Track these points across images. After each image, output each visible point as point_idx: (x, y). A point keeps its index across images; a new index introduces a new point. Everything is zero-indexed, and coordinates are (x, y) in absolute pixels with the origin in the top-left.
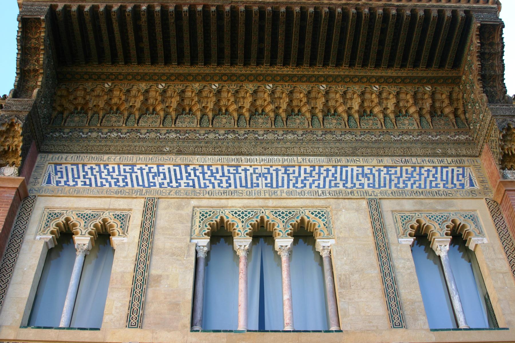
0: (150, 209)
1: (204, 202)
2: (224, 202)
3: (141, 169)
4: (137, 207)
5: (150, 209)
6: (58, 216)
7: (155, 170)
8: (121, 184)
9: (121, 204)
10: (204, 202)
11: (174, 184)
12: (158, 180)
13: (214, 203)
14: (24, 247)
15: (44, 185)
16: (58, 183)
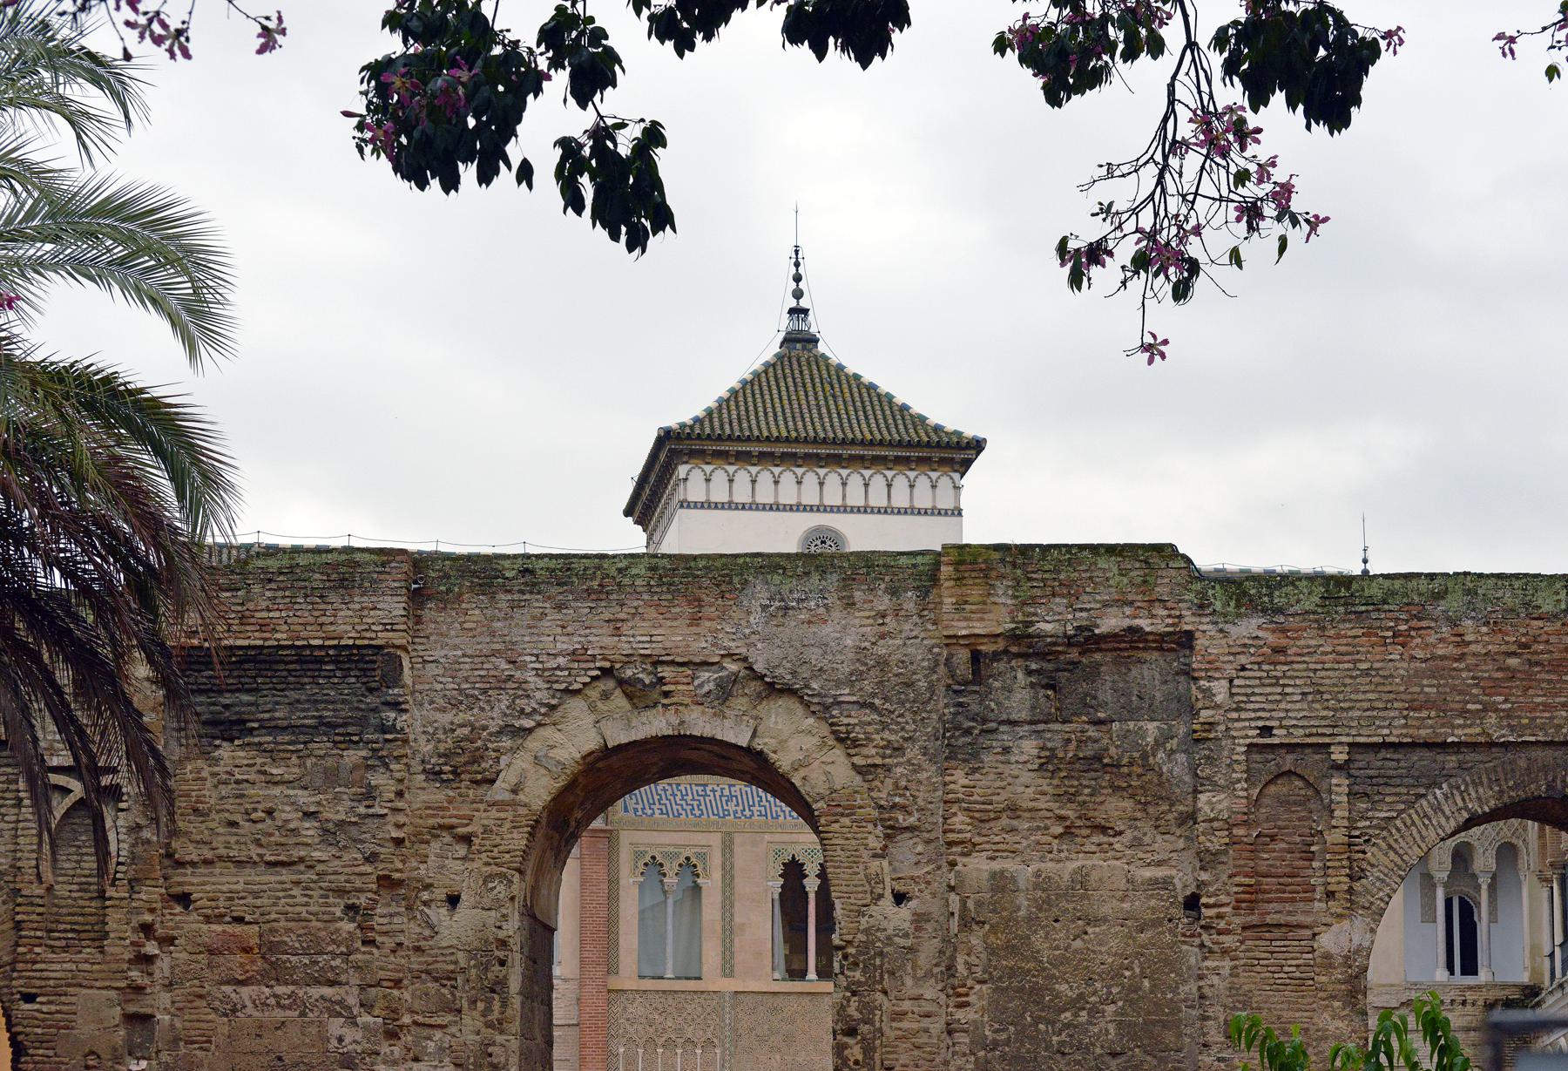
0: (728, 847)
1: (777, 838)
2: (794, 837)
3: (714, 791)
4: (715, 840)
5: (728, 847)
6: (643, 853)
7: (726, 792)
8: (697, 812)
9: (700, 839)
10: (777, 838)
11: (747, 813)
12: (731, 807)
13: (786, 838)
14: (622, 893)
15: (622, 813)
16: (636, 810)
